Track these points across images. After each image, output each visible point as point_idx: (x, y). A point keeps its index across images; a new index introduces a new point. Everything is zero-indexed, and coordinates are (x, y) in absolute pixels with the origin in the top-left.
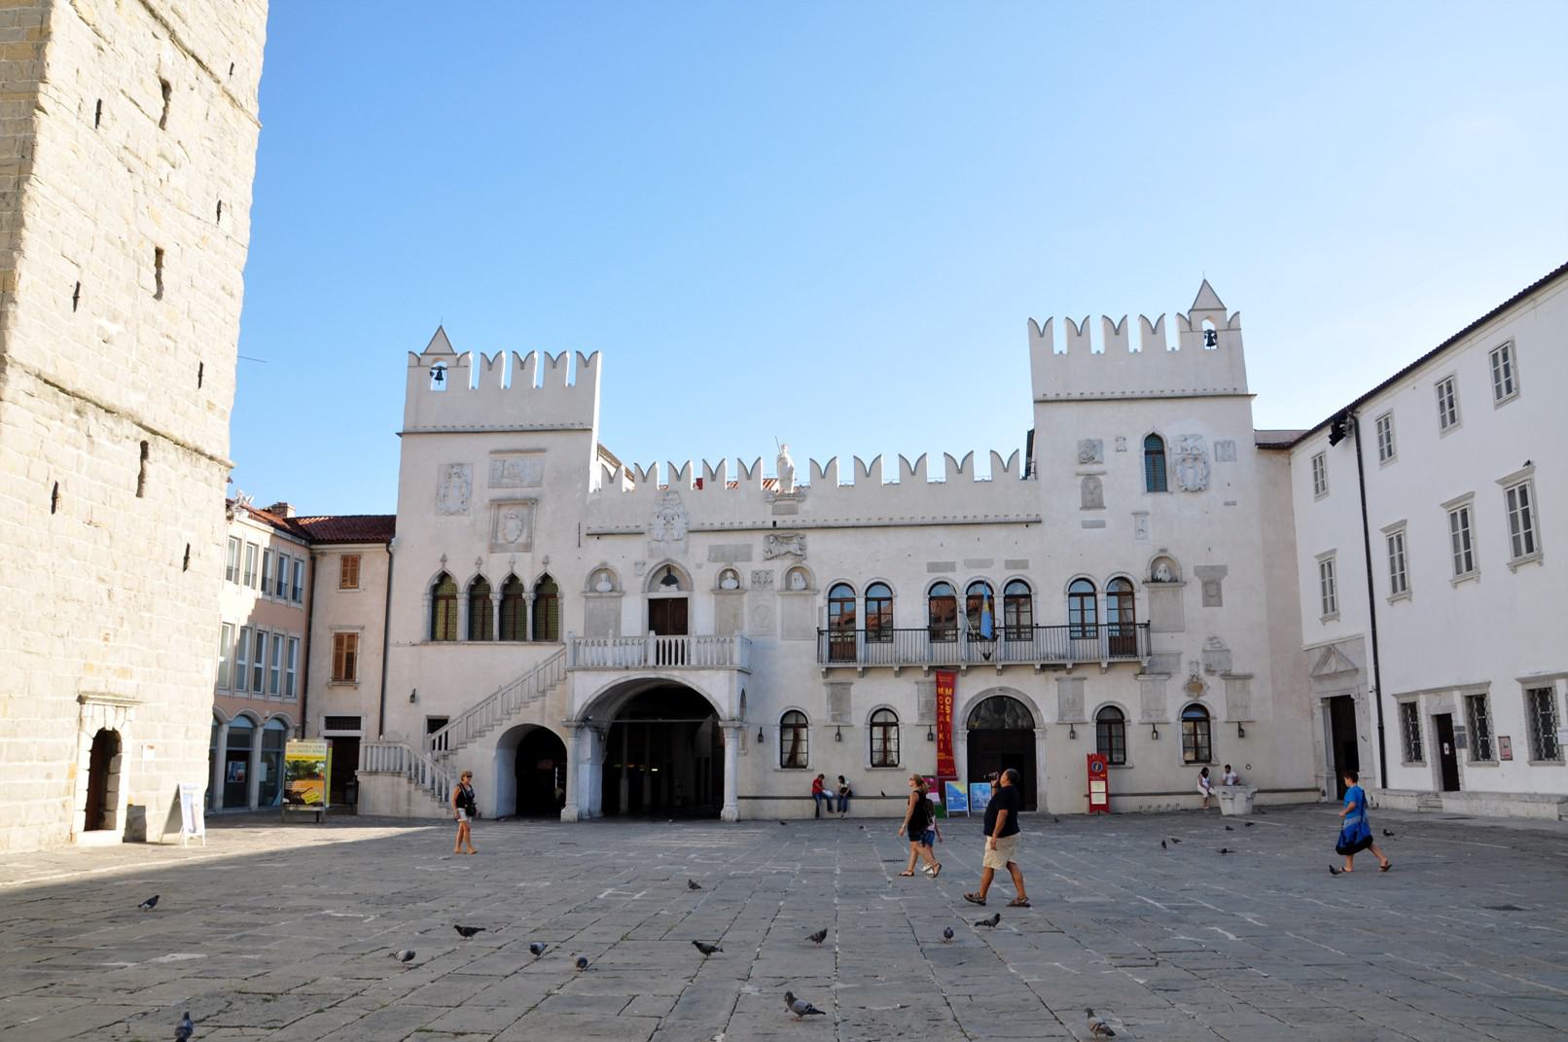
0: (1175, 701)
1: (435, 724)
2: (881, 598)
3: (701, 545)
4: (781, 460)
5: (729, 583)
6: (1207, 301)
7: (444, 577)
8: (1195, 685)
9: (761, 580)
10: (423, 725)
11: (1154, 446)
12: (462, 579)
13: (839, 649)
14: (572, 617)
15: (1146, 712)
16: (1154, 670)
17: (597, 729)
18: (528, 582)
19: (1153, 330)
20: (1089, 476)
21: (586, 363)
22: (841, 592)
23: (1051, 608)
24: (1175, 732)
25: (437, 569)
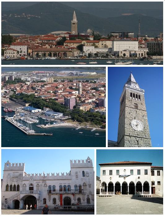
0: (86, 197)
1: (6, 199)
2: (54, 187)
3: (35, 182)
4: (44, 173)
5: (38, 185)
6: (89, 158)
7: (8, 185)
8: (88, 196)
9: (41, 185)
10: (5, 199)
11: (83, 172)
12: (9, 185)
13: (50, 192)
14: (21, 189)
15: (83, 198)
16: (84, 194)
17: (23, 200)
18: (16, 185)
19: (83, 161)
20: (76, 175)
21: (23, 164)
22: (50, 187)
23: (73, 188)
24: (86, 201)
25: (7, 184)
